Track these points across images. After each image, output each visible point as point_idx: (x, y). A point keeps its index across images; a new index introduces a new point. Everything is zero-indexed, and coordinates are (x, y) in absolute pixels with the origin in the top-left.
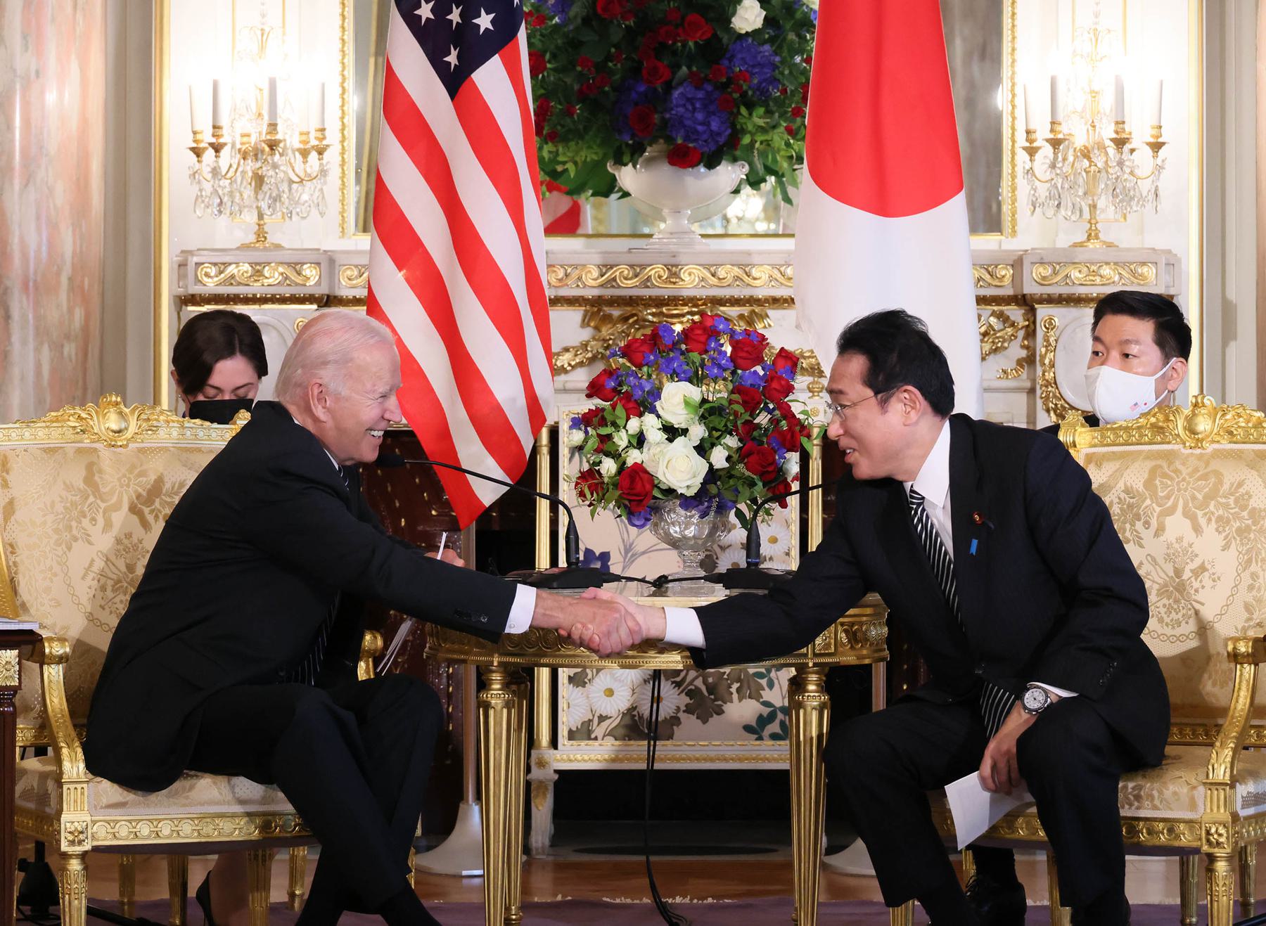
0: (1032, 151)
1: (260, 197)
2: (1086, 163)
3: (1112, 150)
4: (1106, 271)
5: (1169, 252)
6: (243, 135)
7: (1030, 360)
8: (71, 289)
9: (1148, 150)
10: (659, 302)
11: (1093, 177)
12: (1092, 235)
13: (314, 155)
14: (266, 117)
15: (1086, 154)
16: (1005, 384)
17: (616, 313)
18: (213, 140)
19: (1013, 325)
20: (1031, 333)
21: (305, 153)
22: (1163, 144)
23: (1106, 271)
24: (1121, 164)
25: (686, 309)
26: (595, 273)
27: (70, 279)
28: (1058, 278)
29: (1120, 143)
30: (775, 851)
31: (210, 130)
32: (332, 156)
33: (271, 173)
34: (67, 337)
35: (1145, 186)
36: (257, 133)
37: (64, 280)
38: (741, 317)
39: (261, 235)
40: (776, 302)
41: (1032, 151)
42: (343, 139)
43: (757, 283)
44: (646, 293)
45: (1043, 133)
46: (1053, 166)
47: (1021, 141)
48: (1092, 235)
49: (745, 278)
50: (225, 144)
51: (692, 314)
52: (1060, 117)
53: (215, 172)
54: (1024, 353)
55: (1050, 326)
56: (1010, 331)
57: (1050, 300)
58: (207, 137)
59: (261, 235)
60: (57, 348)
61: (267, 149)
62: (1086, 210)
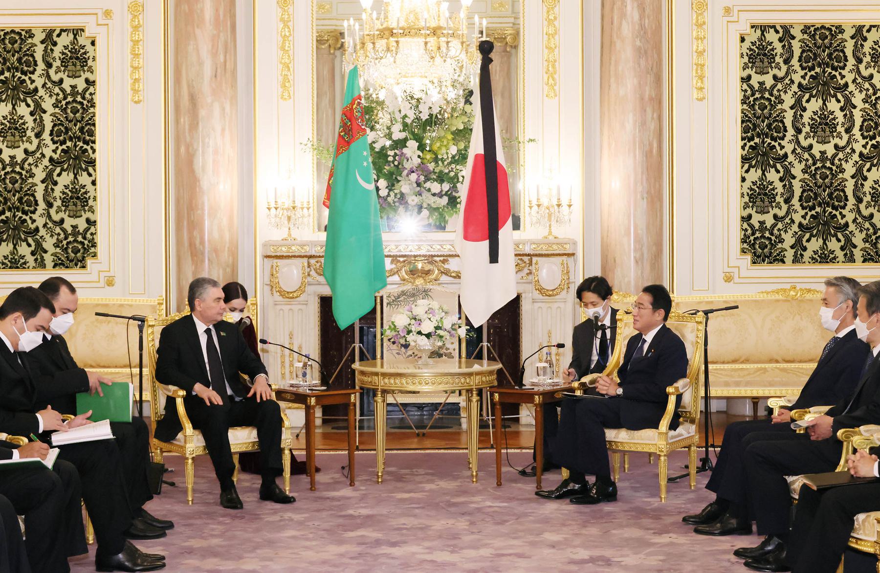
0: (531, 207)
1: (290, 223)
2: (548, 211)
3: (556, 207)
4: (555, 247)
5: (573, 239)
6: (283, 203)
7: (530, 273)
8: (228, 251)
9: (568, 207)
10: (415, 256)
11: (550, 215)
12: (550, 233)
13: (305, 210)
14: (291, 198)
15: (548, 208)
16: (522, 281)
17: (402, 259)
18: (275, 206)
19: (525, 262)
20: (531, 264)
21: (302, 208)
22: (571, 205)
23: (555, 247)
24: (559, 212)
25: (423, 258)
26: (394, 248)
27: (228, 248)
28: (539, 249)
29: (559, 205)
30: (451, 427)
31: (274, 203)
32: (311, 210)
33: (293, 216)
34: (228, 266)
35: (566, 218)
36: (288, 204)
37: (226, 249)
38: (440, 261)
39: (290, 235)
40: (450, 256)
41: (531, 207)
42: (313, 203)
43: (446, 250)
44: (410, 253)
45: (534, 203)
46: (538, 213)
47: (527, 204)
48: (550, 233)
49: (442, 249)
50: (278, 208)
51: (425, 260)
52: (540, 198)
53: (276, 216)
54: (529, 271)
55: (536, 264)
56: (524, 265)
57: (536, 255)
58: (273, 205)
59: (290, 235)
60: (224, 270)
61: (292, 208)
62: (548, 225)
